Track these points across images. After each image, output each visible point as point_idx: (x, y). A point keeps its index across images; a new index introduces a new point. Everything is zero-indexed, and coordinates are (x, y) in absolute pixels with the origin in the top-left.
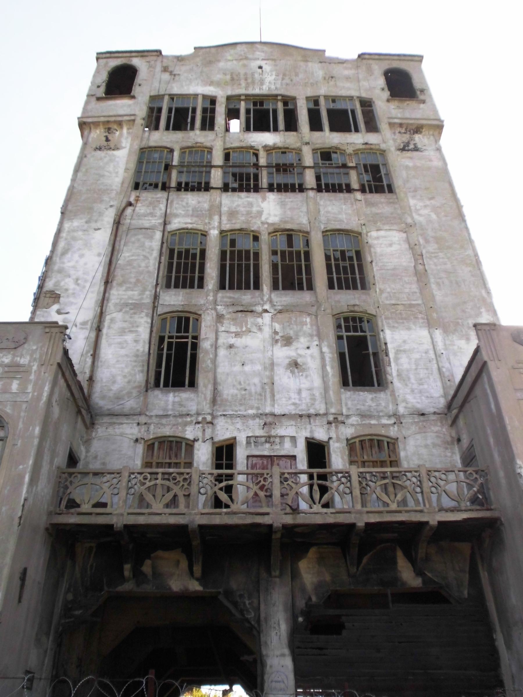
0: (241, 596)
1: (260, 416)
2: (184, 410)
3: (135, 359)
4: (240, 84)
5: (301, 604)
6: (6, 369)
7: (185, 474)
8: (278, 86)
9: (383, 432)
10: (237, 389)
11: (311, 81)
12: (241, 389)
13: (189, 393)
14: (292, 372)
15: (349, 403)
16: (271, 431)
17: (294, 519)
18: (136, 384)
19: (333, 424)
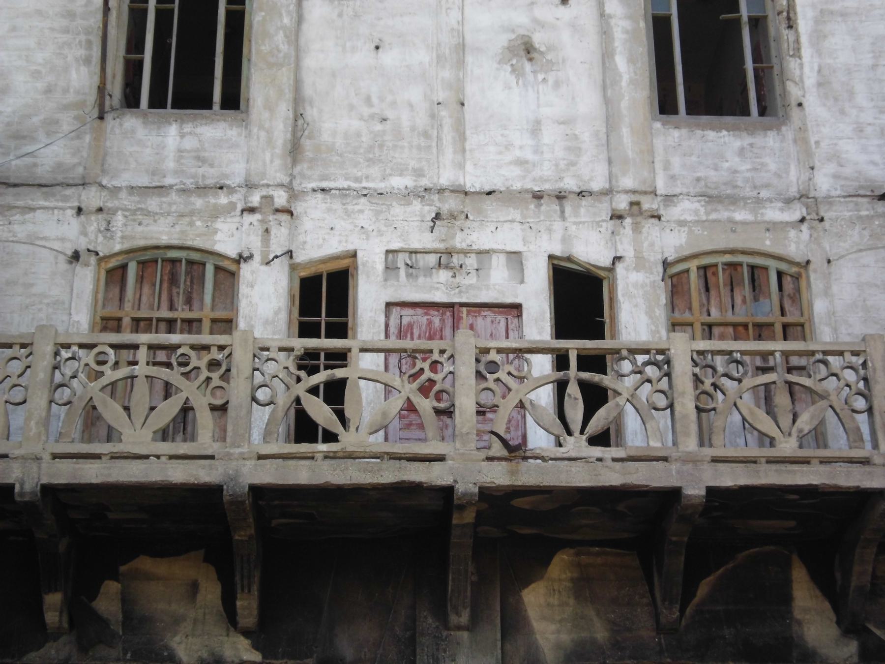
2: (211, 175)
3: (64, 22)
7: (214, 350)
9: (767, 244)
10: (361, 118)
12: (372, 117)
13: (222, 125)
14: (516, 71)
15: (676, 162)
16: (454, 236)
17: (513, 473)
18: (71, 97)
19: (628, 221)
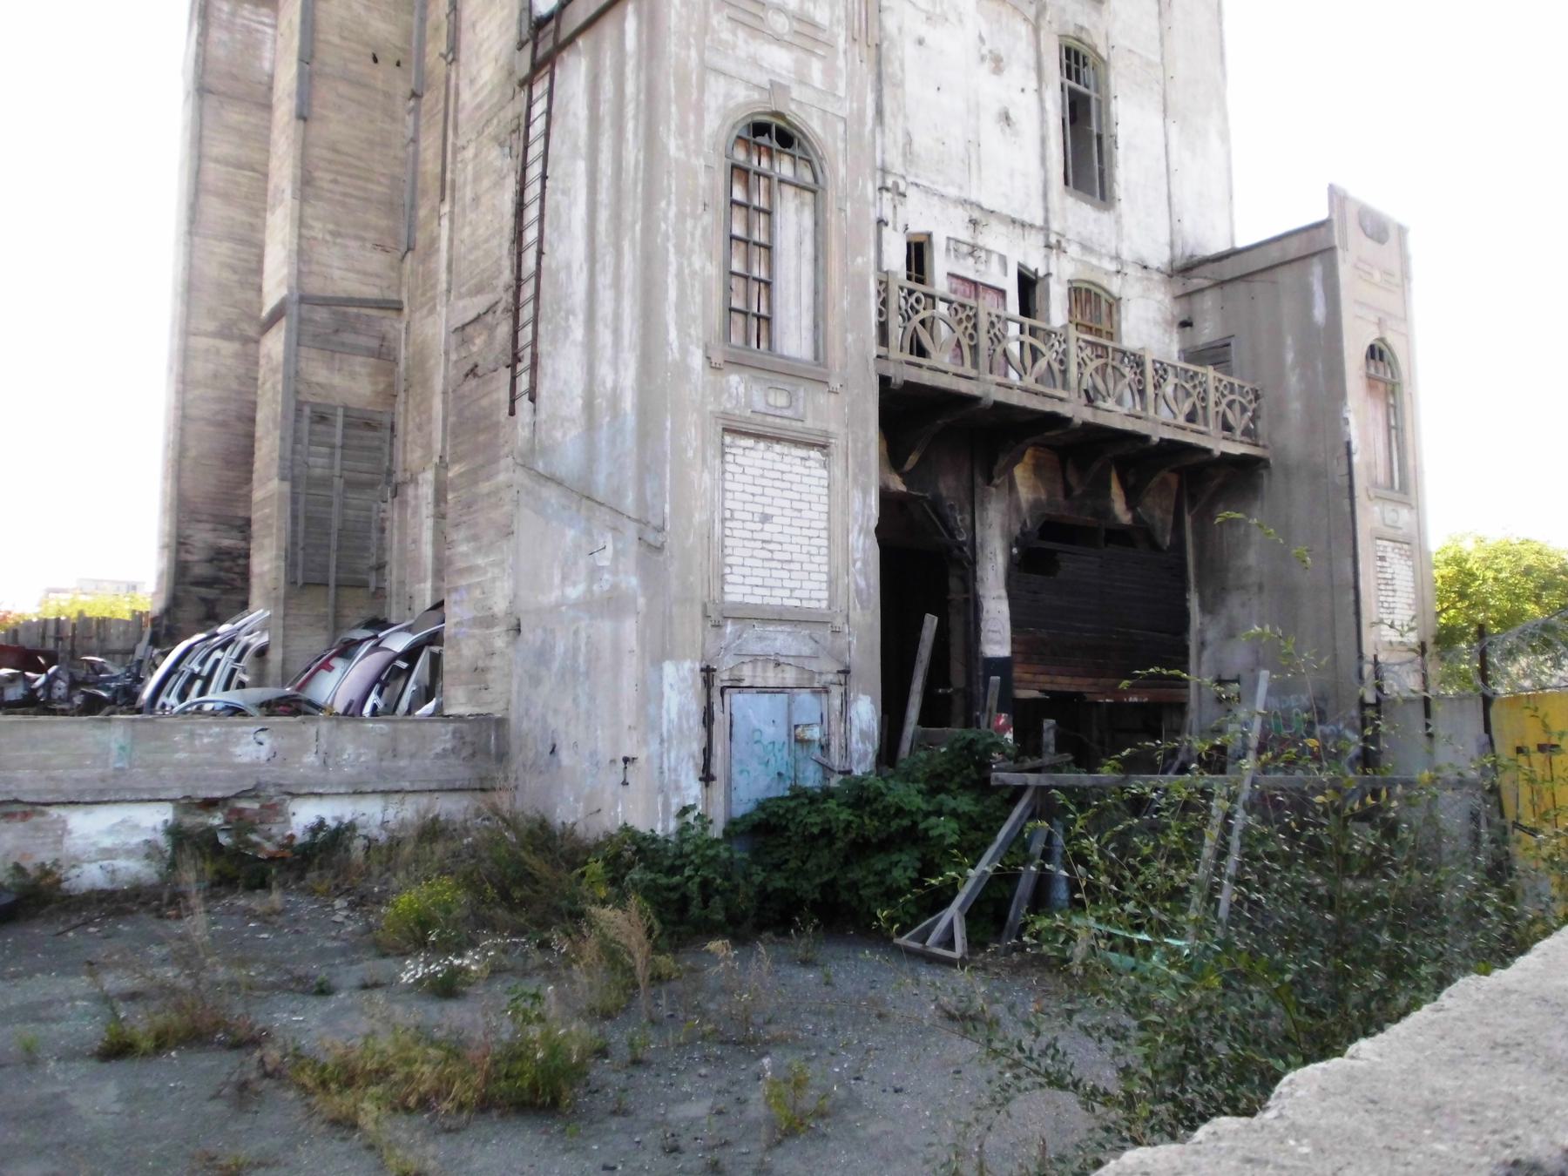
0: (952, 507)
1: (965, 202)
5: (1016, 529)
6: (796, 26)
9: (1104, 282)
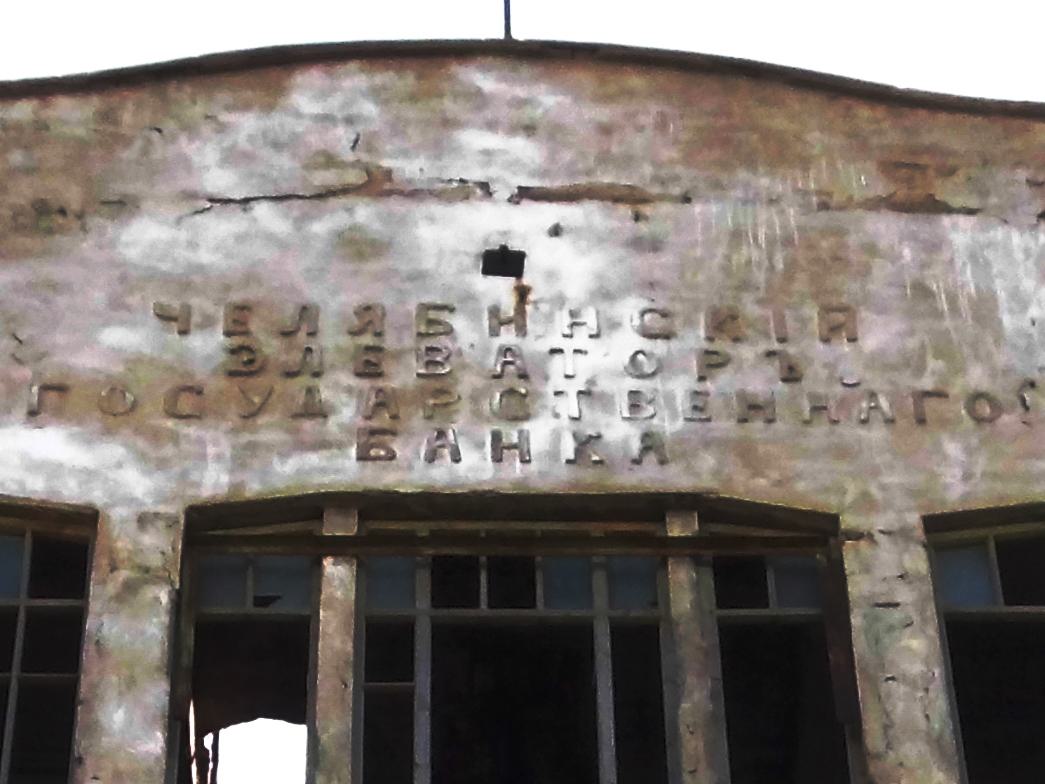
4: (319, 412)
8: (670, 425)
11: (976, 377)
